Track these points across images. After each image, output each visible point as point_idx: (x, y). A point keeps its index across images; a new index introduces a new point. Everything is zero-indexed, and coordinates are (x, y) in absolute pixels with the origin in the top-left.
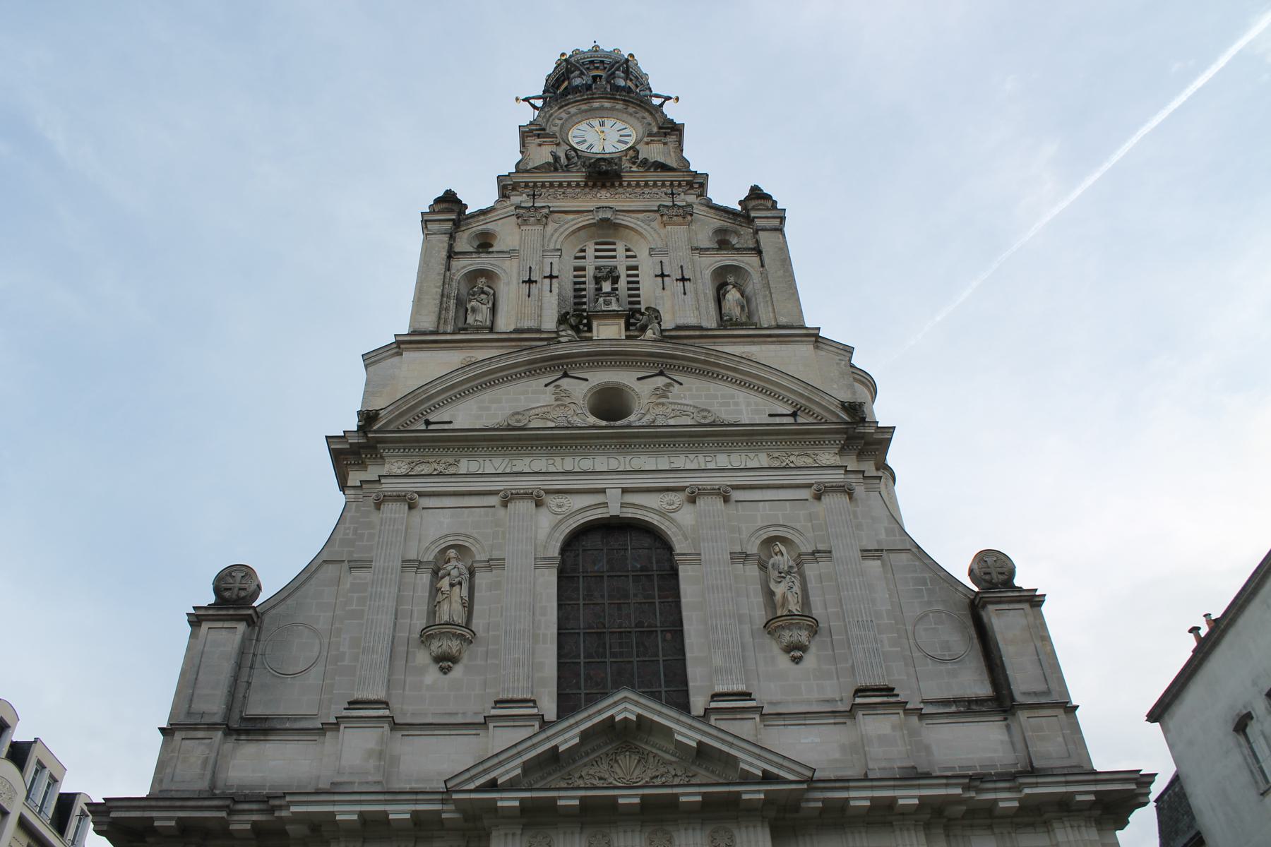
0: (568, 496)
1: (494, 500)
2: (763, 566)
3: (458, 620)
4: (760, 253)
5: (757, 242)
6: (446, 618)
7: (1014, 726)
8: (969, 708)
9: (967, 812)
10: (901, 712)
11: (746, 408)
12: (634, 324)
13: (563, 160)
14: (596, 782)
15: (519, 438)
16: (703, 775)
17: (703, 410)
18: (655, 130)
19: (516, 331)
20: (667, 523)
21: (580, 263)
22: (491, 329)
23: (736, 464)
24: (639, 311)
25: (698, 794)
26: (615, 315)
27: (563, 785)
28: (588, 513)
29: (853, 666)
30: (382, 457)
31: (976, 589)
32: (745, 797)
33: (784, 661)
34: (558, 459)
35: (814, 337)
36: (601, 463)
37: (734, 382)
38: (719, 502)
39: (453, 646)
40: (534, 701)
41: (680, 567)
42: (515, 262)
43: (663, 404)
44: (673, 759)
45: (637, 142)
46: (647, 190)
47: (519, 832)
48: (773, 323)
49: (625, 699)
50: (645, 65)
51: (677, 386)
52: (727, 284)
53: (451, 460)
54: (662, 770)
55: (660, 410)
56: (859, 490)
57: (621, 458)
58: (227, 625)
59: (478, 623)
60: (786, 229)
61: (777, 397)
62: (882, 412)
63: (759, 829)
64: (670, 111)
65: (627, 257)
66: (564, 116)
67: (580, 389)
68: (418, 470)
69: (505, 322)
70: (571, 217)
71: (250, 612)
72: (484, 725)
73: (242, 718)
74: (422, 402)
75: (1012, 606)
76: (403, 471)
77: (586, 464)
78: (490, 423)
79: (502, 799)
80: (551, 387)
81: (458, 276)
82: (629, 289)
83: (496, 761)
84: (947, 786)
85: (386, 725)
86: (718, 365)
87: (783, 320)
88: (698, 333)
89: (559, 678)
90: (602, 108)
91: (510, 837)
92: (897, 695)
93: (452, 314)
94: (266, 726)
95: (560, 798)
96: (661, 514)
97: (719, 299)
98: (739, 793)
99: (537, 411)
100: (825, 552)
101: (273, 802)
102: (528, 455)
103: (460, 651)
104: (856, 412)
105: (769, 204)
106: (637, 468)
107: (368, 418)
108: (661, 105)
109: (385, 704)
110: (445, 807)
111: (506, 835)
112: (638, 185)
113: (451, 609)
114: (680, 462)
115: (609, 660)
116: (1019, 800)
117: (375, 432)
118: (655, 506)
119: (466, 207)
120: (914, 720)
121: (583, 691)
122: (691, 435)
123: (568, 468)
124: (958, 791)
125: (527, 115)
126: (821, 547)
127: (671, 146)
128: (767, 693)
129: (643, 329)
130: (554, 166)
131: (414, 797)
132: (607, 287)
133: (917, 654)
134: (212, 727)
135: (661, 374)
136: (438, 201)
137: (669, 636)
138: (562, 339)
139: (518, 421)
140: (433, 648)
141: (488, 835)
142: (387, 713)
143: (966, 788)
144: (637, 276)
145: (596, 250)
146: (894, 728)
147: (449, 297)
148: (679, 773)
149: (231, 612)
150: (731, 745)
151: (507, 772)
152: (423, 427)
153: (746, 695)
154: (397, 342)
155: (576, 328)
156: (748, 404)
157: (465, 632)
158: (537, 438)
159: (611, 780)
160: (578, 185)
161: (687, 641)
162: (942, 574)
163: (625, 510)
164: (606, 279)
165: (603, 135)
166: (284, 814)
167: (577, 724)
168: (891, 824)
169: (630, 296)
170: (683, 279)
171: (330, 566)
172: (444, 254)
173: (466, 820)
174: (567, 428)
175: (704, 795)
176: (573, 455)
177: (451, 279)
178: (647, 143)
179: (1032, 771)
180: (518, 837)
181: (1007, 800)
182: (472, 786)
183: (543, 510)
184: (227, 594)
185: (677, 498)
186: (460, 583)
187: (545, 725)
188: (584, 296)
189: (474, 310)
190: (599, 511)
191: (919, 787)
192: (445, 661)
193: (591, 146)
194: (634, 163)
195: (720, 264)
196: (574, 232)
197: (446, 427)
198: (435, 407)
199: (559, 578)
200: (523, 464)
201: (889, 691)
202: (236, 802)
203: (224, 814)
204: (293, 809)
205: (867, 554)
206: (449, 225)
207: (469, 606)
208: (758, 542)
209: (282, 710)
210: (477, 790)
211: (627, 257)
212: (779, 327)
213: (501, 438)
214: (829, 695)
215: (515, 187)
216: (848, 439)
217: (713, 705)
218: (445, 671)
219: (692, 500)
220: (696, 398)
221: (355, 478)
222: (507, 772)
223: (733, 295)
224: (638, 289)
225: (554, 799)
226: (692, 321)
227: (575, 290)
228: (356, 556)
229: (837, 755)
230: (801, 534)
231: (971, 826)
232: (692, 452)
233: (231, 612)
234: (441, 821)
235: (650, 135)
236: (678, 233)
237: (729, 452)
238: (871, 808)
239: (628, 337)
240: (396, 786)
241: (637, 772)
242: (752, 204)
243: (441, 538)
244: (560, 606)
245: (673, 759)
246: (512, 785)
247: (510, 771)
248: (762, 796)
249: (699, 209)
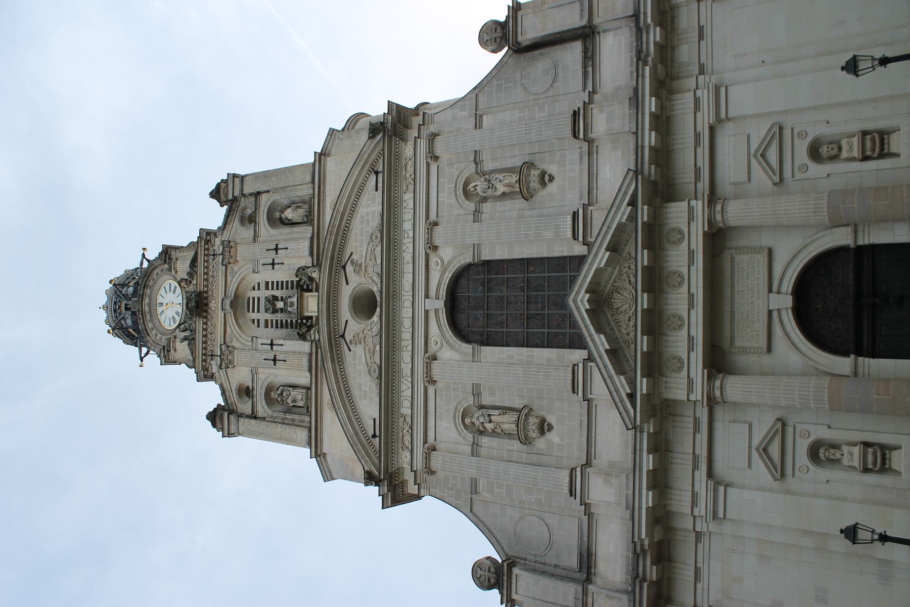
0: (430, 337)
1: (431, 390)
2: (484, 200)
3: (515, 418)
4: (259, 193)
5: (251, 195)
6: (513, 426)
7: (604, 27)
8: (589, 58)
9: (662, 64)
10: (591, 106)
11: (371, 206)
12: (308, 286)
13: (187, 333)
14: (632, 323)
15: (387, 371)
16: (630, 248)
17: (371, 238)
18: (166, 266)
19: (310, 371)
20: (451, 267)
21: (262, 323)
22: (309, 389)
23: (411, 216)
24: (298, 282)
25: (642, 252)
26: (300, 300)
27: (633, 346)
28: (442, 323)
29: (558, 139)
30: (398, 469)
31: (506, 48)
32: (646, 219)
33: (552, 188)
34: (403, 343)
35: (321, 156)
36: (407, 313)
37: (351, 216)
38: (438, 230)
39: (533, 421)
40: (574, 365)
41: (483, 258)
42: (260, 370)
43: (366, 267)
44: (617, 269)
45: (175, 279)
46: (211, 274)
47: (664, 379)
48: (310, 185)
49: (574, 301)
50: (118, 272)
51: (353, 257)
52: (281, 218)
53: (402, 420)
54: (625, 276)
55: (370, 269)
56: (433, 128)
57: (404, 298)
58: (514, 581)
59: (518, 404)
60: (242, 174)
61: (363, 185)
62: (377, 110)
63: (668, 210)
64: (152, 255)
65: (259, 289)
66: (154, 332)
67: (353, 326)
68: (408, 444)
69: (304, 378)
70: (228, 329)
71: (505, 564)
72: (589, 401)
73: (579, 571)
74: (359, 440)
75: (519, 24)
76: (408, 454)
77: (407, 323)
78: (375, 391)
79: (641, 390)
80: (351, 347)
81: (269, 412)
82: (282, 288)
83: (614, 394)
84: (643, 77)
85: (588, 470)
86: (339, 226)
87: (308, 178)
88: (315, 240)
89: (558, 347)
90: (149, 304)
91: (668, 385)
92: (579, 109)
93: (296, 417)
94: (585, 554)
95: (642, 349)
96: (444, 271)
97: (292, 224)
98: (643, 223)
99: (368, 357)
100: (475, 155)
101: (638, 551)
102: (400, 365)
103: (537, 417)
104: (376, 129)
105: (223, 185)
106: (411, 287)
107: (370, 479)
108: (148, 261)
109: (573, 470)
110: (646, 430)
111: (666, 388)
112: (207, 280)
113: (507, 422)
114: (408, 257)
115: (546, 312)
116: (655, 26)
117: (380, 474)
118: (439, 275)
119: (219, 405)
120: (596, 97)
121: (568, 331)
122: (389, 247)
123: (409, 336)
124: (647, 69)
125: (153, 359)
126: (472, 158)
127: (179, 254)
128: (574, 201)
129: (311, 279)
130: (191, 340)
131: (638, 452)
132: (280, 305)
133: (550, 93)
134: (585, 592)
135: (344, 267)
136: (214, 425)
137: (531, 269)
138: (317, 338)
139: (375, 371)
140: (534, 436)
141: (666, 400)
142: (579, 469)
143: (645, 63)
144: (273, 283)
145: (253, 311)
146: (602, 112)
147: (284, 419)
148: (627, 265)
149: (505, 578)
150: (609, 227)
151: (623, 386)
152: (377, 439)
153: (575, 215)
154: (316, 457)
155: (310, 328)
156: (368, 206)
157: (523, 413)
158: (387, 357)
159: (631, 313)
160: (205, 323)
161: (535, 256)
162: (495, 72)
163: (441, 297)
164: (274, 305)
165: (169, 304)
166: (646, 543)
167: (591, 336)
168: (668, 118)
169: (287, 288)
170: (276, 249)
171: (475, 507)
172: (253, 421)
173: (654, 416)
174: (381, 336)
175: (643, 248)
176: (400, 333)
177: (271, 417)
178: (176, 272)
179: (636, 16)
180: (668, 380)
181: (655, 35)
182: (632, 411)
183: (439, 355)
184: (493, 581)
185: (433, 259)
186: (489, 415)
187: (590, 358)
188: (286, 321)
189: (294, 401)
190: (441, 315)
191: (643, 96)
192: (544, 427)
193: (177, 313)
194: (190, 282)
195: (266, 222)
196: (239, 327)
197: (377, 423)
198: (363, 430)
199: (487, 345)
200: (406, 368)
201: (575, 114)
202: (637, 576)
203: (645, 585)
204: (643, 536)
205: (478, 125)
206: (232, 417)
207: (505, 410)
208: (467, 202)
209: (574, 544)
210: (634, 408)
211: (259, 289)
212: (313, 182)
213: (387, 383)
214: (577, 156)
215: (205, 369)
216: (395, 135)
217: (581, 239)
218: (551, 427)
219: (435, 248)
220: (362, 243)
221: (412, 489)
222: (623, 386)
223: (289, 214)
224: (282, 282)
225: (642, 353)
226: (307, 244)
227: (282, 327)
228: (468, 489)
229: (619, 153)
230: (462, 171)
231: (672, 61)
232: (401, 247)
233: (505, 578)
234: (655, 433)
235: (170, 270)
236: (243, 252)
237: (403, 221)
238: (657, 131)
239: (317, 290)
240: (630, 464)
241: (626, 294)
242: (223, 198)
243: (457, 429)
244: (507, 345)
245: (617, 269)
246: (632, 383)
247: (622, 383)
248: (646, 207)
249: (226, 236)
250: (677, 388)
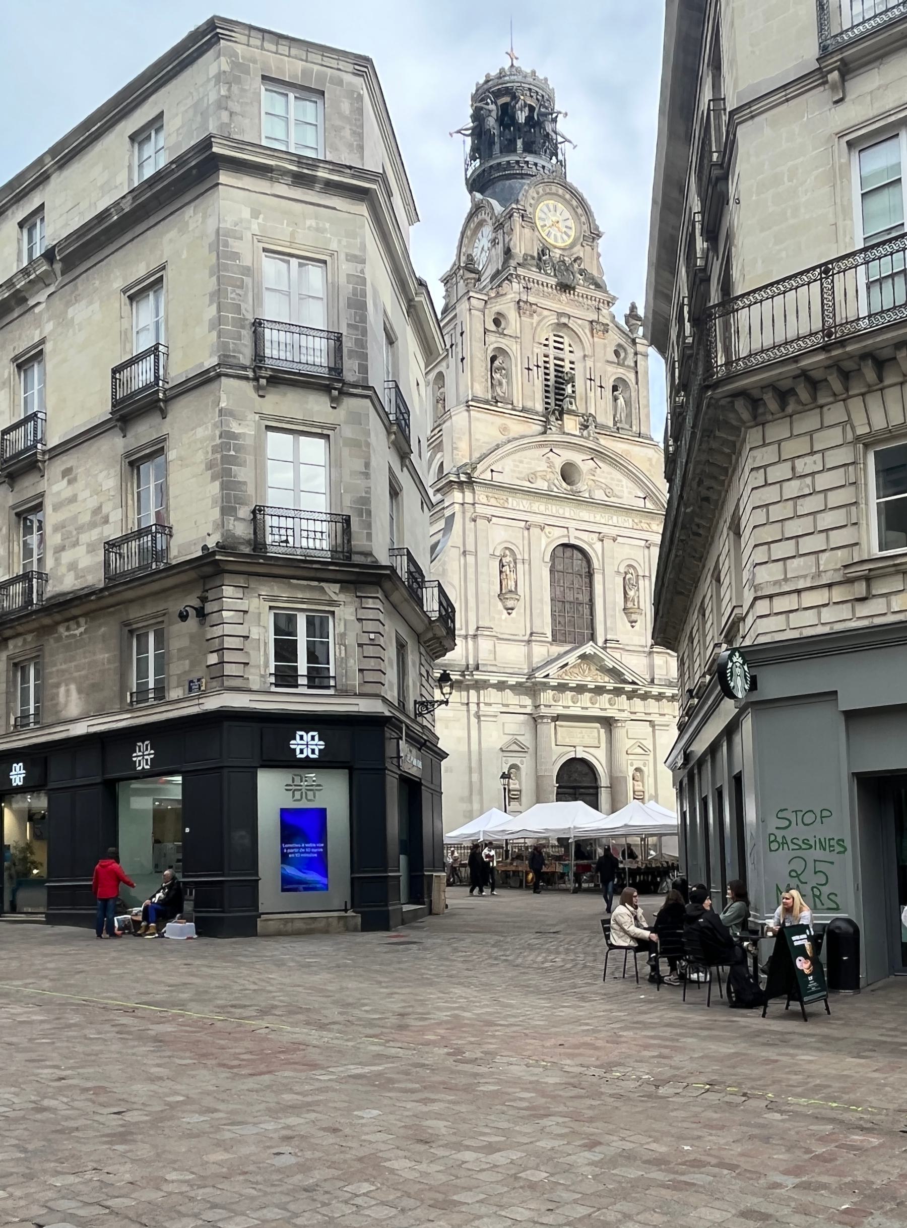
67: (558, 463)
70: (546, 313)
170: (601, 387)
250: (546, 697)
